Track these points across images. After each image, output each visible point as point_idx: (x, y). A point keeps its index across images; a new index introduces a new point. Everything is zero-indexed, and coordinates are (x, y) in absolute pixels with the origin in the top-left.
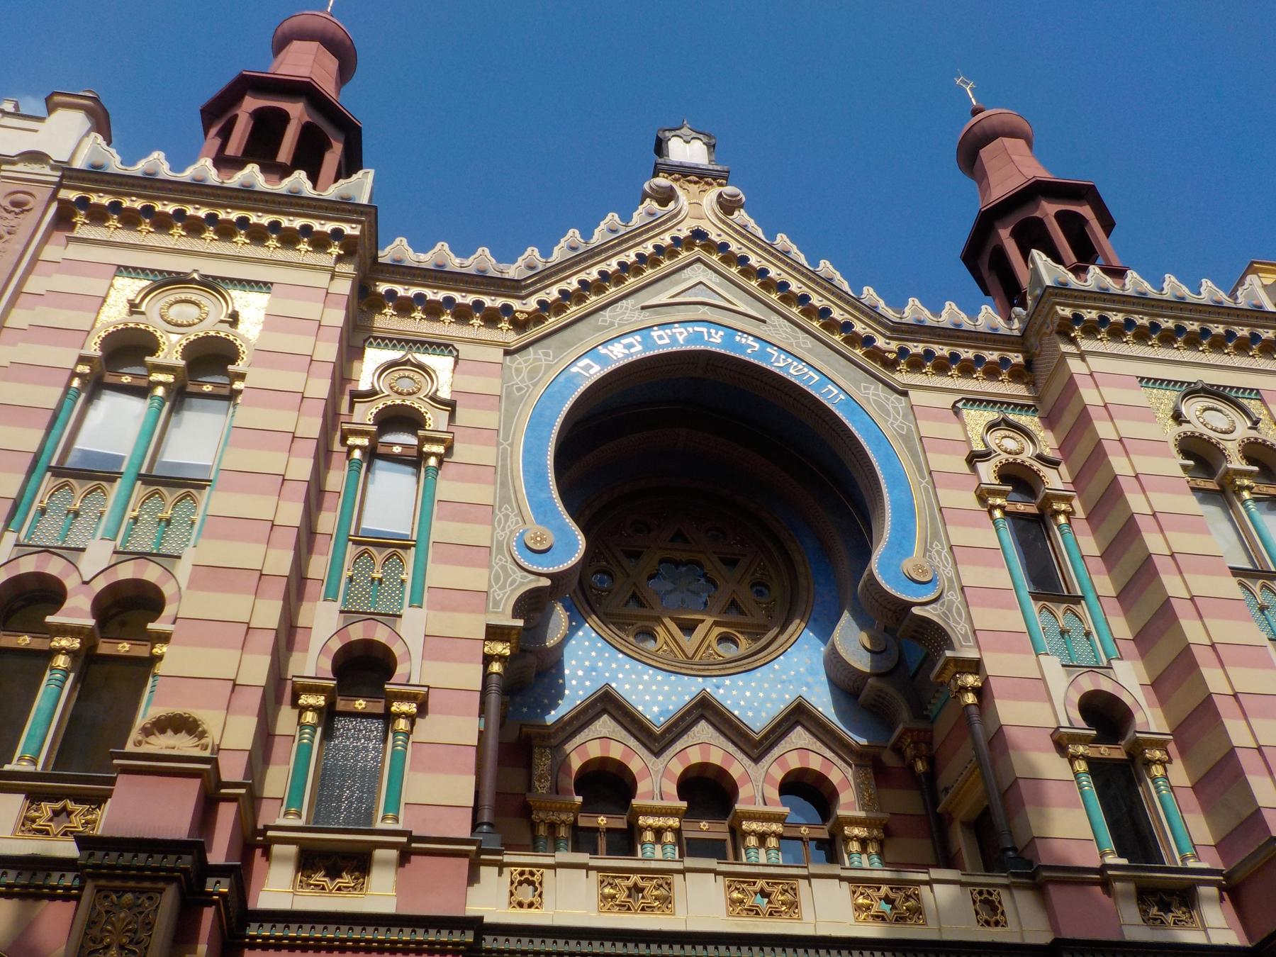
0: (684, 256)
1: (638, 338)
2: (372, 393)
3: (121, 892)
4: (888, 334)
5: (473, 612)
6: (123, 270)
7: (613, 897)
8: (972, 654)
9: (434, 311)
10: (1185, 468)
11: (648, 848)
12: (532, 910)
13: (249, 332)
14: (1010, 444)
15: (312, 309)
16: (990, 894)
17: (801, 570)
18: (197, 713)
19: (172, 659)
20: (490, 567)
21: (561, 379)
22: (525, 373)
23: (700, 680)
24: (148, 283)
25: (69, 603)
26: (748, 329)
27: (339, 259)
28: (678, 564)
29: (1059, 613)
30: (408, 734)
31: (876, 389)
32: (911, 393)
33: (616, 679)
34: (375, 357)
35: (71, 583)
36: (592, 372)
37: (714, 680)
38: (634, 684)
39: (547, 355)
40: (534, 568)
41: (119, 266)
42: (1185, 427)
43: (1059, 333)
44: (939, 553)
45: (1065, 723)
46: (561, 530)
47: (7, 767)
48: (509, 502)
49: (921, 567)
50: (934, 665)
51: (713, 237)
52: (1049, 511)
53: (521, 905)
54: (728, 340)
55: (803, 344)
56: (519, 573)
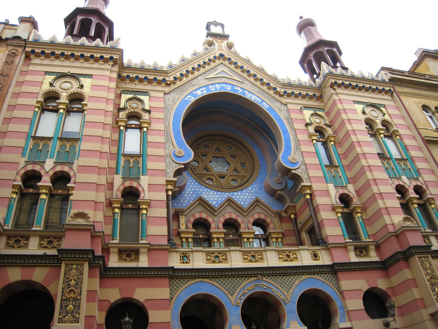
0: (218, 62)
2: (124, 109)
3: (72, 265)
4: (281, 87)
5: (162, 176)
6: (47, 73)
8: (309, 184)
9: (141, 81)
10: (366, 128)
11: (216, 244)
12: (187, 264)
13: (87, 91)
14: (317, 121)
15: (106, 83)
16: (315, 252)
17: (255, 159)
18: (86, 211)
19: (76, 195)
20: (166, 162)
21: (182, 102)
22: (171, 100)
24: (55, 77)
25: (43, 179)
26: (238, 85)
27: (112, 65)
28: (218, 158)
29: (333, 171)
30: (146, 215)
31: (278, 104)
32: (288, 105)
33: (202, 194)
34: (125, 97)
35: (43, 173)
36: (192, 99)
38: (208, 195)
39: (177, 94)
40: (179, 162)
41: (45, 72)
42: (366, 116)
43: (331, 87)
45: (335, 203)
46: (186, 150)
47: (33, 229)
49: (294, 158)
50: (298, 188)
51: (226, 56)
52: (328, 141)
53: (184, 263)
54: (232, 89)
55: (255, 90)
56: (174, 164)
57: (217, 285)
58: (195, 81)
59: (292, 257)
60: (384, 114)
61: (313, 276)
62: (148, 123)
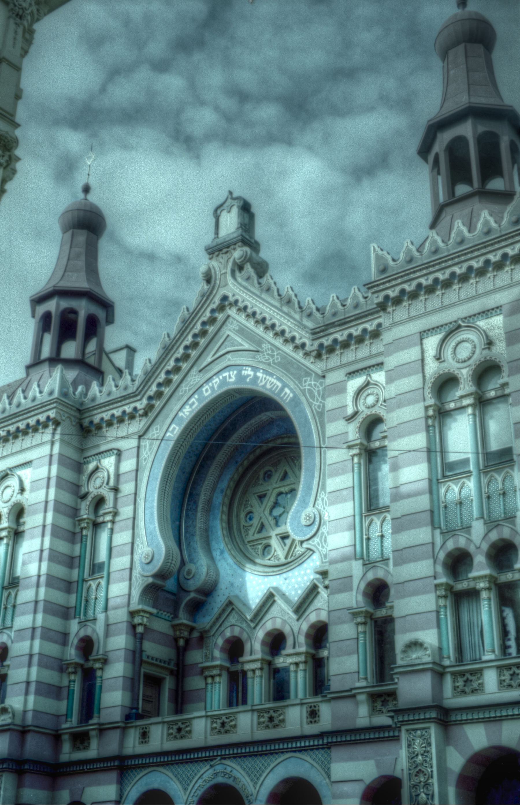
0: (220, 317)
1: (196, 396)
4: (311, 337)
7: (172, 734)
14: (371, 400)
16: (315, 707)
23: (278, 577)
30: (101, 677)
37: (284, 575)
39: (157, 429)
44: (323, 499)
48: (139, 538)
57: (170, 774)
58: (183, 385)
59: (276, 721)
60: (490, 343)
61: (298, 755)
62: (110, 512)
